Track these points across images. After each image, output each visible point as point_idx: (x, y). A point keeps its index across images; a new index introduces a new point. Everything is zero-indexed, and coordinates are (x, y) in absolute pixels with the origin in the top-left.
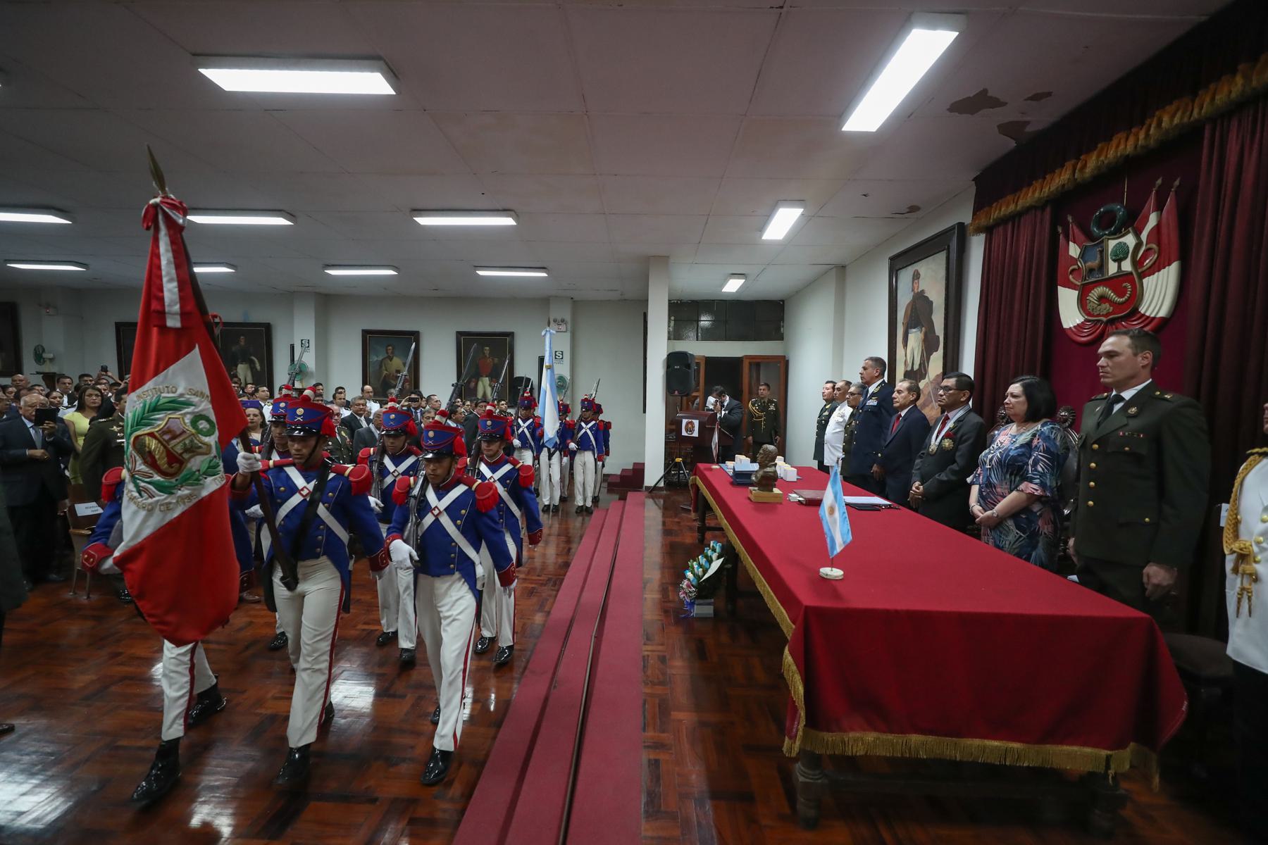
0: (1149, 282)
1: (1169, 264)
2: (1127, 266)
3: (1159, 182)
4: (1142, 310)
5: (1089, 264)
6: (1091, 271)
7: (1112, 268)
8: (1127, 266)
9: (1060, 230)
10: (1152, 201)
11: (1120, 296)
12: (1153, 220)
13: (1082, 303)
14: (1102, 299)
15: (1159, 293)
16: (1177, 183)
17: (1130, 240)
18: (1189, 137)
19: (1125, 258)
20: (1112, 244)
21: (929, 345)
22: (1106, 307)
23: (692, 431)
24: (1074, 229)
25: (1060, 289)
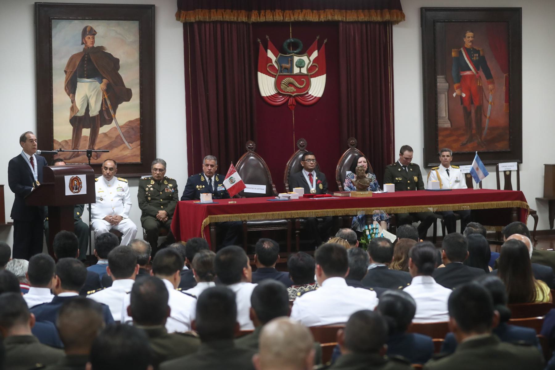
0: (312, 80)
1: (323, 74)
2: (304, 71)
3: (318, 37)
4: (310, 93)
5: (284, 65)
6: (286, 69)
7: (296, 70)
8: (304, 71)
9: (259, 40)
10: (315, 44)
11: (300, 85)
12: (315, 54)
13: (278, 85)
14: (291, 84)
15: (317, 87)
16: (325, 41)
17: (305, 58)
18: (335, 24)
19: (303, 67)
20: (296, 59)
21: (116, 94)
22: (292, 89)
23: (78, 188)
24: (270, 43)
25: (260, 74)
